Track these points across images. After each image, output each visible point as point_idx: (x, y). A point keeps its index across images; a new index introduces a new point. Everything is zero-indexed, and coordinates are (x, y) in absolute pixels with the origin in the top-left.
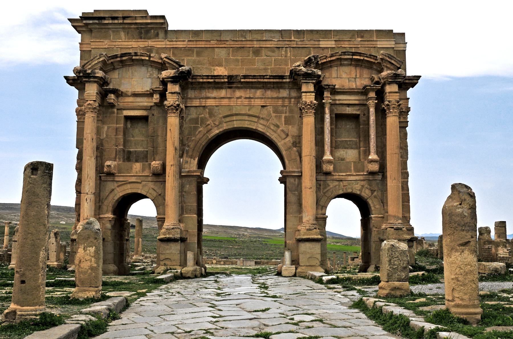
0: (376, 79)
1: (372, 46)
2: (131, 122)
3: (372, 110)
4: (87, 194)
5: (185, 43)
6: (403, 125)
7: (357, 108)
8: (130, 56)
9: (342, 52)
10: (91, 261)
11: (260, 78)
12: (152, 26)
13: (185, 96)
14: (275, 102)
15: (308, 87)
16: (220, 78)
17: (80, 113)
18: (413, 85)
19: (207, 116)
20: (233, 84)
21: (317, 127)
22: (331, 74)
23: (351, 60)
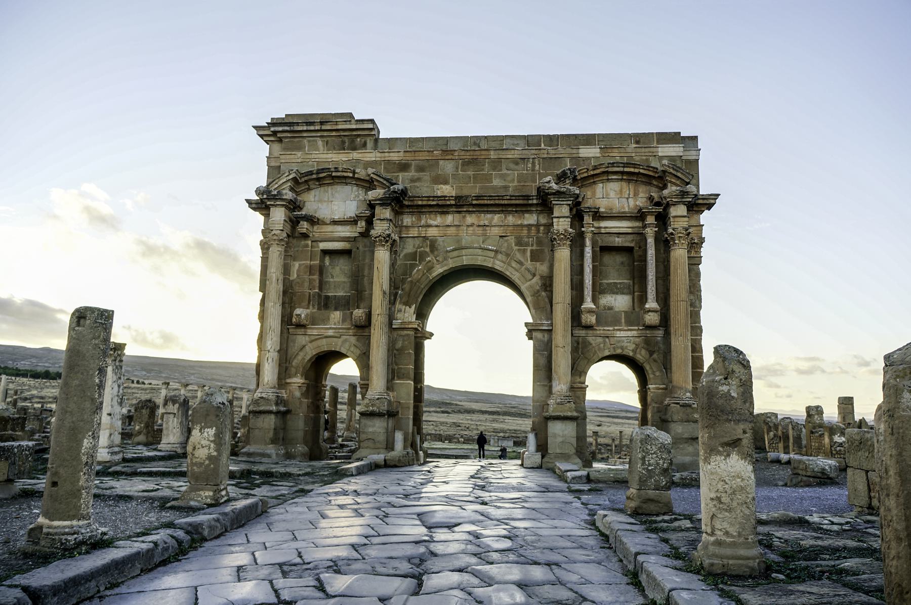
0: (656, 199)
1: (650, 154)
2: (330, 257)
3: (651, 241)
4: (269, 351)
5: (401, 154)
6: (694, 262)
7: (630, 237)
8: (329, 172)
9: (609, 164)
10: (209, 448)
11: (498, 199)
12: (359, 133)
13: (400, 223)
14: (519, 231)
15: (562, 210)
16: (445, 200)
17: (265, 246)
18: (709, 206)
19: (428, 250)
20: (463, 208)
21: (574, 264)
22: (594, 194)
23: (622, 173)
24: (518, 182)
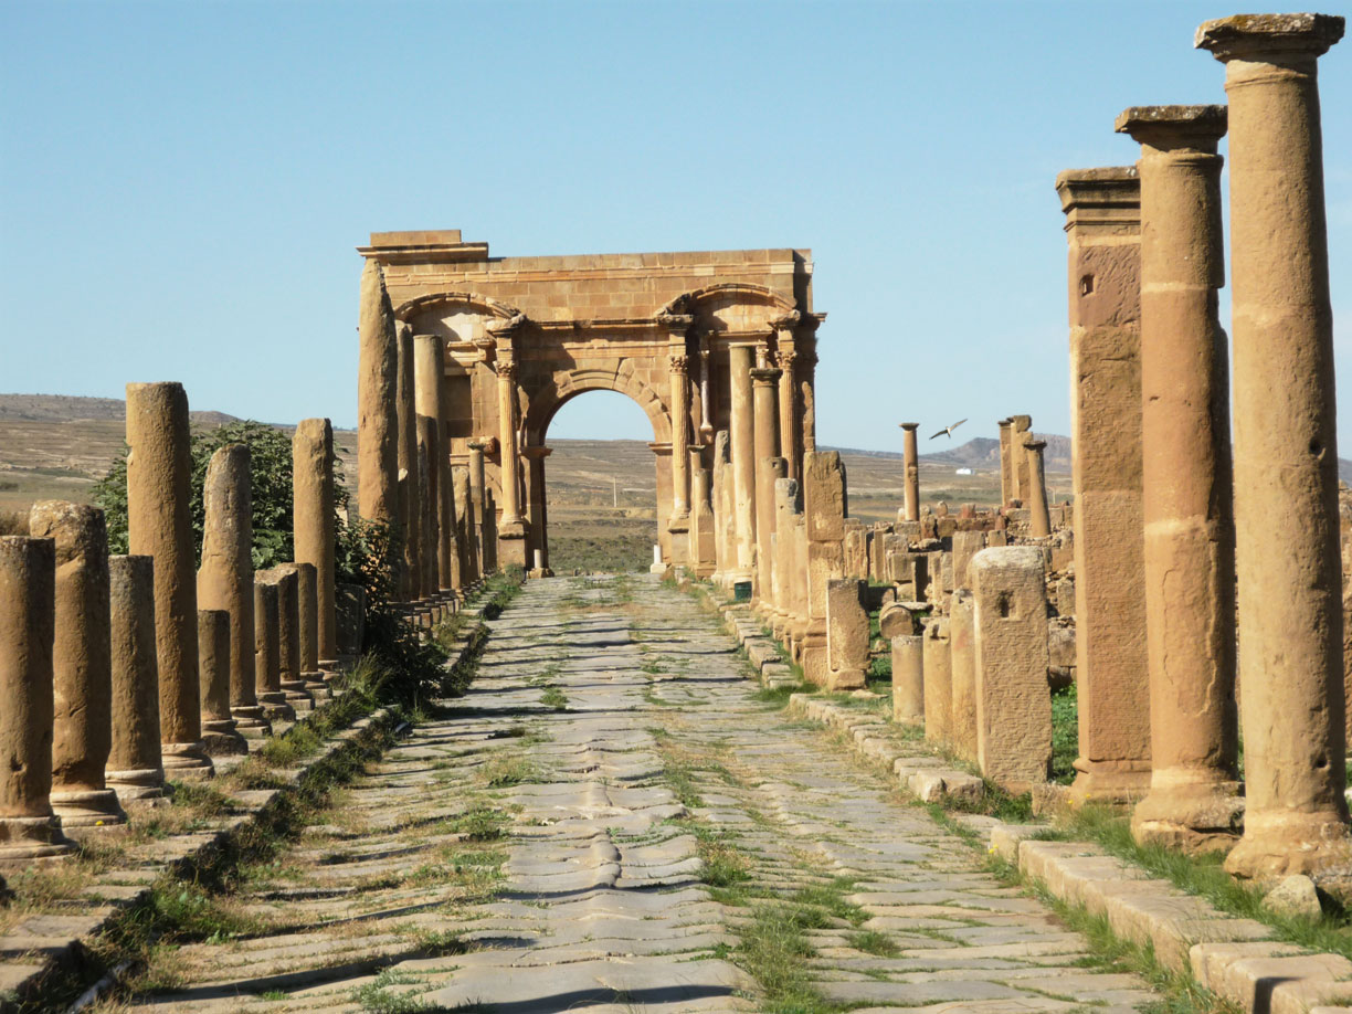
24: (636, 303)
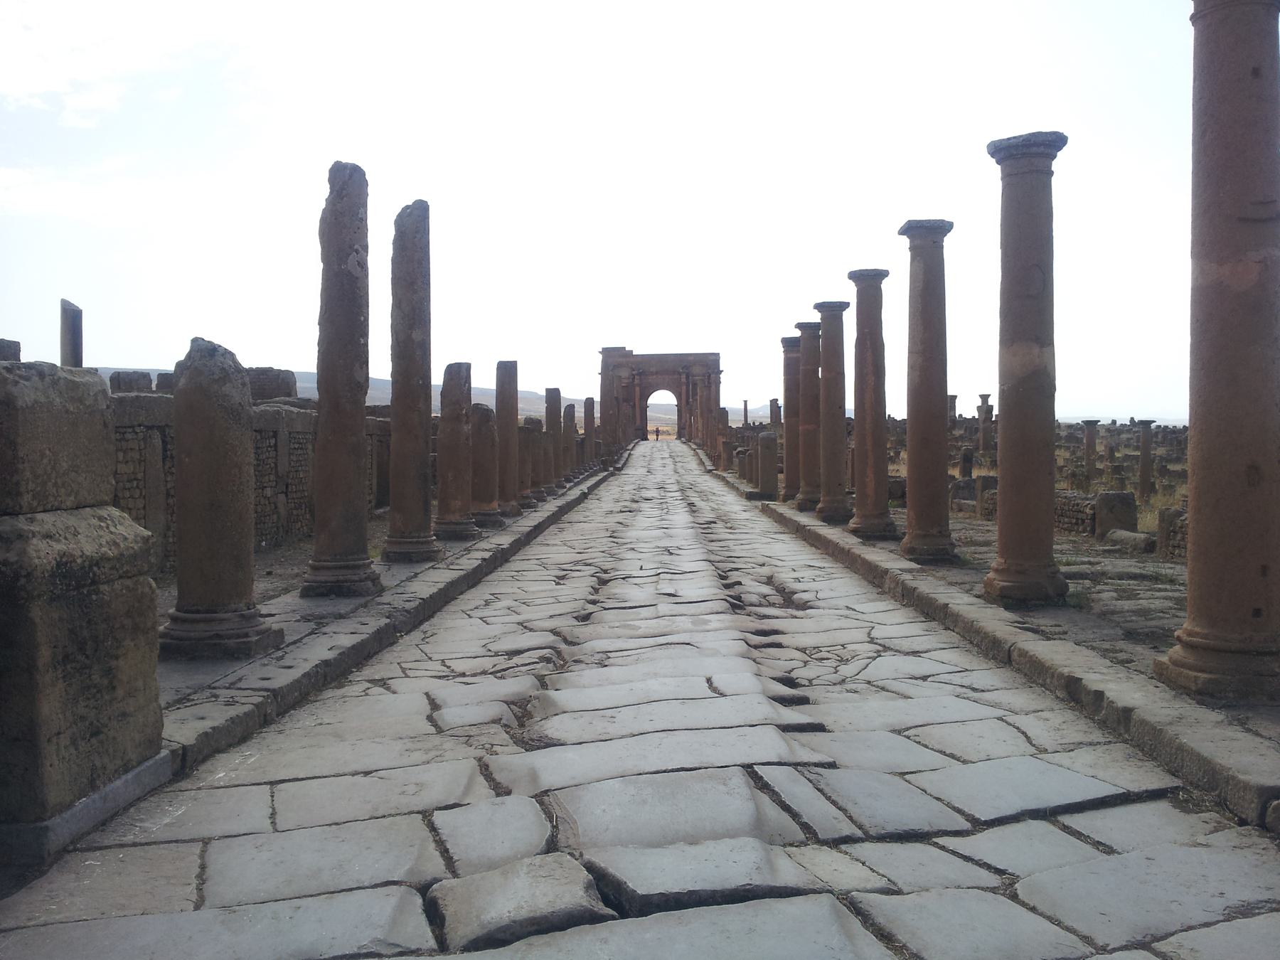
15: (684, 376)
